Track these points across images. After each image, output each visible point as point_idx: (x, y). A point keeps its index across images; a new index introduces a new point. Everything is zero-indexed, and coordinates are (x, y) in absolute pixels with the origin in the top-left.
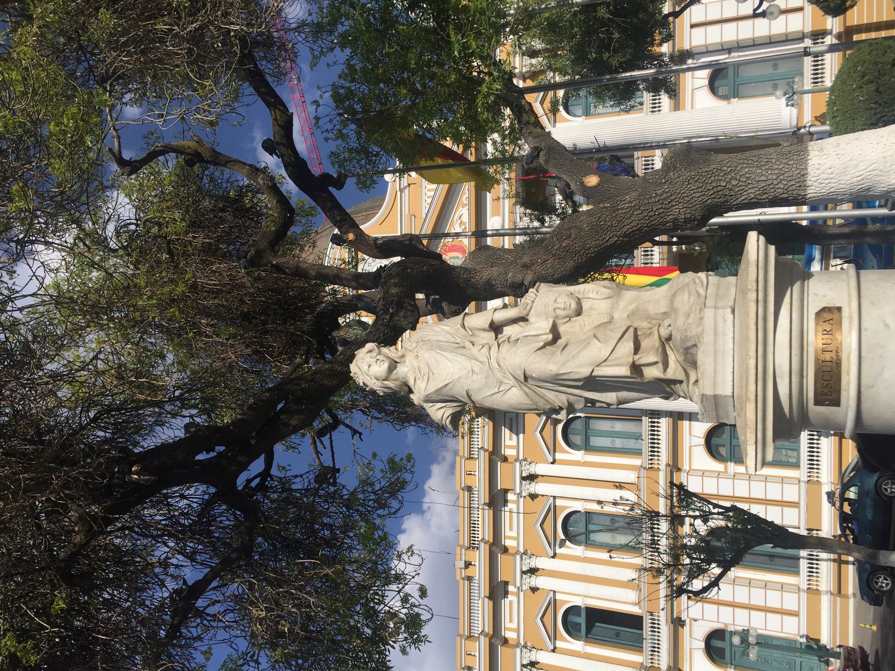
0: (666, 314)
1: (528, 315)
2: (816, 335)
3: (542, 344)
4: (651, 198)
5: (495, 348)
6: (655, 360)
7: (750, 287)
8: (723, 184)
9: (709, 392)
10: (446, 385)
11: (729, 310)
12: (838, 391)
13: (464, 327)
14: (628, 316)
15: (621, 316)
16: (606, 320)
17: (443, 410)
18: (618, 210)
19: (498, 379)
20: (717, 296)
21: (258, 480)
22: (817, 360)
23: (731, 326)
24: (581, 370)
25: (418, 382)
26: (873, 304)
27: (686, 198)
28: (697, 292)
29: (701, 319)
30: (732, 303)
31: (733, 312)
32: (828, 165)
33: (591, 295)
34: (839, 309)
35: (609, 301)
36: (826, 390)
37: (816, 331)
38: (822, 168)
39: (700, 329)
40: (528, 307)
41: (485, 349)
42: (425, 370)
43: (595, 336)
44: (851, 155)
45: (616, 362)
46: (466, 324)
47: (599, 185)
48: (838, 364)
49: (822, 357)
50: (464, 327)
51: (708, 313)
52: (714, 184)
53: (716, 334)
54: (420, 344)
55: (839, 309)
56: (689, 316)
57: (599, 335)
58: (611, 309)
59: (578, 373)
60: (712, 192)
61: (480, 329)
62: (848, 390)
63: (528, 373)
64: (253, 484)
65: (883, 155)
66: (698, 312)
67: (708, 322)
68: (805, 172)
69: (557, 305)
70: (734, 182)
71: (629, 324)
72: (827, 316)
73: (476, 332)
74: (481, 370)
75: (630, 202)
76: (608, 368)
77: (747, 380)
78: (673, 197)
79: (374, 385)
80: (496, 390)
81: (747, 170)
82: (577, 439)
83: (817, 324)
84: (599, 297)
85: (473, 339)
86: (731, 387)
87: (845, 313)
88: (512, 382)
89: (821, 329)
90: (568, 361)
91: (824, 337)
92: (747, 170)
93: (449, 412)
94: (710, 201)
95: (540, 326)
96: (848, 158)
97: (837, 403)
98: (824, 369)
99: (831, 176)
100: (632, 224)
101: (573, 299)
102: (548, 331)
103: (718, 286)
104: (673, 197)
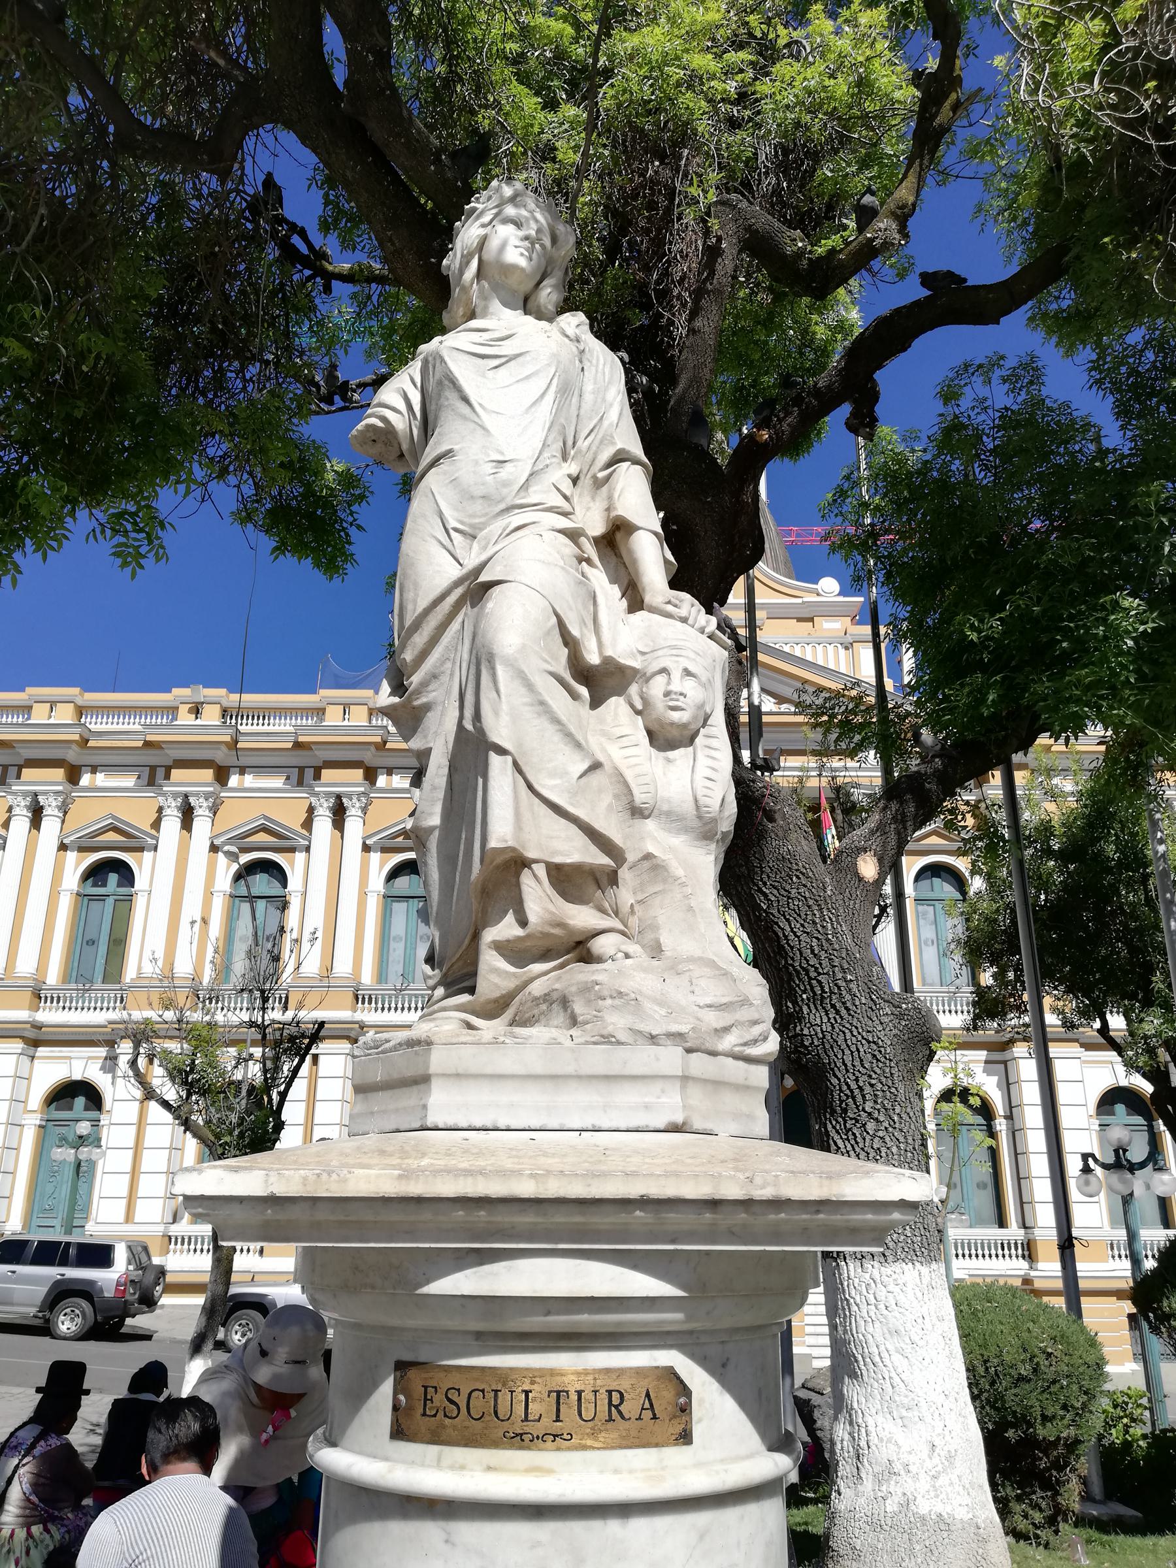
0: (656, 950)
1: (653, 610)
2: (607, 1371)
3: (575, 631)
4: (844, 971)
5: (564, 523)
6: (532, 918)
7: (758, 1180)
8: (868, 1106)
9: (438, 1060)
10: (466, 400)
11: (679, 1118)
12: (436, 1438)
13: (619, 458)
14: (648, 857)
15: (654, 838)
16: (639, 797)
17: (402, 406)
18: (821, 910)
19: (481, 527)
20: (717, 1084)
21: (304, 249)
22: (534, 1375)
23: (633, 1124)
24: (505, 719)
25: (476, 337)
26: (702, 1537)
27: (841, 1037)
28: (727, 1029)
29: (653, 1039)
30: (698, 1125)
31: (675, 1128)
32: (902, 1299)
33: (702, 761)
34: (685, 1437)
35: (689, 808)
36: (439, 1399)
37: (620, 1372)
38: (896, 1289)
39: (622, 1036)
40: (670, 608)
41: (560, 502)
42: (507, 348)
43: (596, 766)
44: (921, 1343)
45: (526, 815)
46: (625, 465)
47: (861, 879)
48: (519, 1440)
49: (537, 1390)
50: (619, 458)
51: (670, 1058)
52: (868, 1089)
53: (608, 1078)
54: (573, 347)
55: (685, 1437)
56: (661, 1004)
57: (596, 778)
58: (668, 814)
59: (496, 713)
60: (853, 1086)
61: (610, 497)
62: (438, 1464)
63: (496, 590)
64: (296, 240)
65: (923, 1403)
66: (675, 1028)
67: (643, 1058)
68: (890, 1258)
69: (676, 674)
70: (871, 1126)
71: (631, 857)
72: (665, 1399)
73: (605, 489)
74: (506, 484)
75: (835, 934)
76: (508, 790)
77: (468, 1173)
78: (843, 1012)
79: (468, 234)
80: (452, 523)
81: (894, 1150)
82: (403, 883)
83: (640, 1372)
84: (700, 783)
85: (586, 481)
86: (451, 1122)
87: (674, 1455)
88: (471, 562)
89: (624, 1385)
90: (530, 686)
91: (603, 1397)
92: (894, 1150)
93: (399, 422)
94: (835, 1081)
95: (620, 636)
96: (916, 1338)
97: (399, 1433)
98: (504, 1397)
99: (882, 1307)
100: (792, 936)
101: (695, 718)
102: (609, 652)
103: (743, 1088)
104: (843, 1012)
